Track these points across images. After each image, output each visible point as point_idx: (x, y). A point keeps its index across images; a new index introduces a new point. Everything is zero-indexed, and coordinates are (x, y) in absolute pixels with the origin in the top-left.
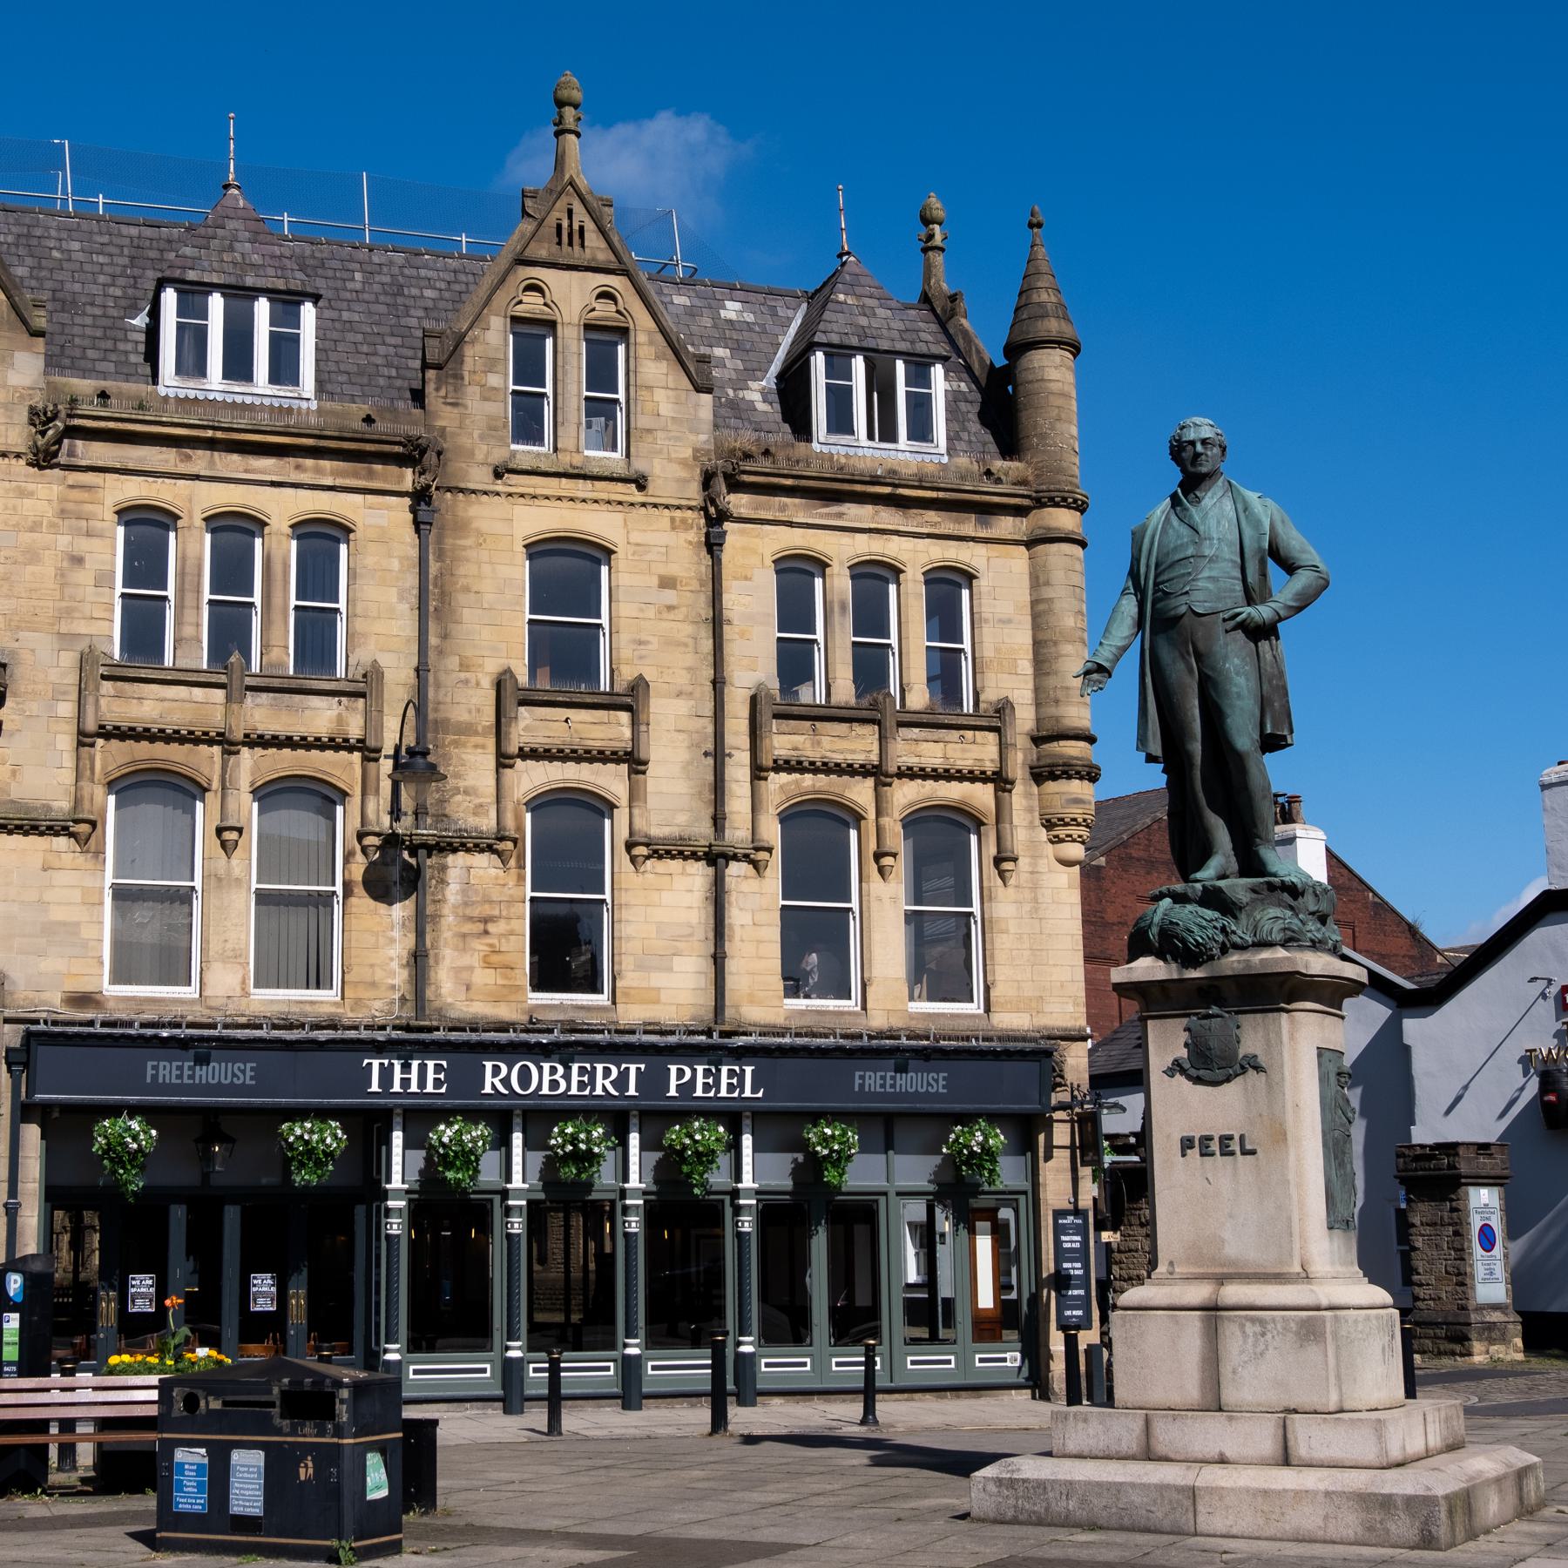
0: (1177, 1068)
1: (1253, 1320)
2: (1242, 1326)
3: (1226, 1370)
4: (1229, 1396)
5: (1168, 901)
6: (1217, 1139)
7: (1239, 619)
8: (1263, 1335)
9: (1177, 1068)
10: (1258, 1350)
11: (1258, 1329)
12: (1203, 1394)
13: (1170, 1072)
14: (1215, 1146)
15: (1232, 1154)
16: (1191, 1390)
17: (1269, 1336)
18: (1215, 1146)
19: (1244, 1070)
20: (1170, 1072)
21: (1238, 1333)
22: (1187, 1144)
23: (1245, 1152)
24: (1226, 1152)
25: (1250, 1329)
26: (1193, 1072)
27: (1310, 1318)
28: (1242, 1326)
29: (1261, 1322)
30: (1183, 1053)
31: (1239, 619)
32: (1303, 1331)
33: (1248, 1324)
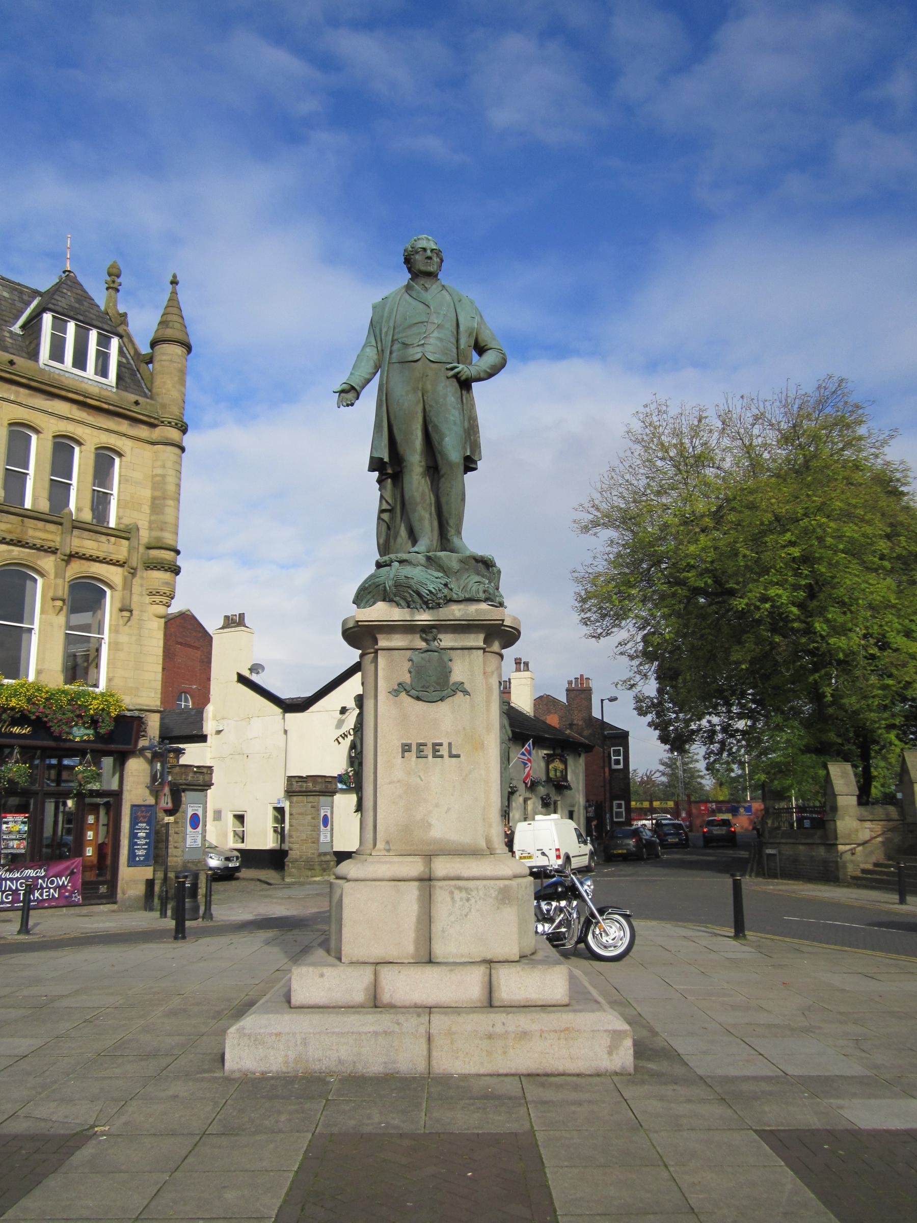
0: (401, 689)
1: (460, 889)
2: (452, 893)
3: (437, 928)
4: (440, 950)
5: (396, 564)
6: (430, 746)
7: (456, 370)
8: (468, 900)
9: (401, 689)
10: (464, 913)
11: (464, 895)
12: (417, 949)
13: (395, 693)
14: (428, 751)
15: (441, 757)
16: (407, 946)
17: (473, 900)
18: (428, 751)
19: (454, 693)
20: (395, 693)
21: (449, 899)
22: (406, 748)
23: (452, 756)
24: (436, 754)
25: (458, 895)
26: (413, 692)
27: (506, 886)
28: (452, 893)
29: (467, 890)
30: (407, 678)
31: (456, 370)
32: (500, 897)
33: (456, 892)
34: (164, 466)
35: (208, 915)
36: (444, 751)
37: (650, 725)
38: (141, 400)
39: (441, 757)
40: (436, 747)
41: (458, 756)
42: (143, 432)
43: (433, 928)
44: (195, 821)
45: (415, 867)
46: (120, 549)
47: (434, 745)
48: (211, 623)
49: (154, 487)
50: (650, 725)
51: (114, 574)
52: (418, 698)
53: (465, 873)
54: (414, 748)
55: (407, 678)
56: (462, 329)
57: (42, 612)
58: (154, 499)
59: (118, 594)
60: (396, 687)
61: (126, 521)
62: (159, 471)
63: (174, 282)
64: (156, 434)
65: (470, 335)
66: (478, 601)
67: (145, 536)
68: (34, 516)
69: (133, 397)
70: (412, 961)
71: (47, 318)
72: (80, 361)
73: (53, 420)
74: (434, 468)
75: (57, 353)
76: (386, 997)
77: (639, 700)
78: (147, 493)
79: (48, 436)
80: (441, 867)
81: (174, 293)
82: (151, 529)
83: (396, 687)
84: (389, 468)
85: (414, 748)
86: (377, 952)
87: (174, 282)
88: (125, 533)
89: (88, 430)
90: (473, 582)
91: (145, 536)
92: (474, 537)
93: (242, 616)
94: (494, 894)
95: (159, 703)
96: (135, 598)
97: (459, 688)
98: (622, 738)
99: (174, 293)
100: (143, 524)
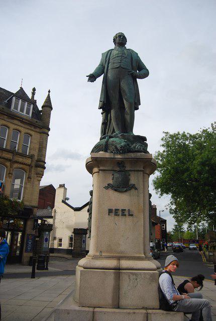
4: (123, 302)
11: (135, 277)
15: (125, 215)
16: (109, 300)
17: (138, 280)
18: (120, 213)
22: (110, 211)
24: (123, 215)
29: (135, 274)
32: (151, 278)
33: (131, 275)
34: (43, 139)
35: (47, 269)
36: (127, 213)
37: (173, 217)
38: (38, 121)
39: (125, 215)
40: (123, 210)
41: (132, 215)
42: (38, 130)
43: (121, 293)
44: (47, 240)
45: (112, 263)
46: (28, 161)
47: (122, 210)
48: (56, 186)
49: (40, 145)
50: (173, 217)
51: (27, 168)
52: (116, 190)
53: (135, 267)
54: (114, 211)
55: (111, 182)
56: (133, 59)
57: (6, 177)
58: (40, 148)
59: (27, 174)
60: (107, 185)
61: (31, 153)
62: (41, 141)
63: (49, 92)
64: (41, 131)
65: (137, 62)
66: (141, 152)
67: (36, 158)
68: (6, 150)
69: (36, 120)
70: (110, 307)
71: (14, 98)
72: (22, 110)
74: (122, 107)
75: (16, 108)
77: (171, 209)
78: (37, 146)
81: (49, 94)
82: (38, 156)
83: (107, 185)
84: (106, 106)
85: (114, 211)
86: (95, 302)
87: (49, 92)
88: (31, 157)
89: (23, 128)
90: (138, 146)
91: (36, 158)
92: (137, 131)
93: (64, 184)
94: (148, 277)
95: (37, 205)
96: (32, 175)
97: (133, 187)
98: (164, 222)
99: (49, 94)
100: (36, 155)
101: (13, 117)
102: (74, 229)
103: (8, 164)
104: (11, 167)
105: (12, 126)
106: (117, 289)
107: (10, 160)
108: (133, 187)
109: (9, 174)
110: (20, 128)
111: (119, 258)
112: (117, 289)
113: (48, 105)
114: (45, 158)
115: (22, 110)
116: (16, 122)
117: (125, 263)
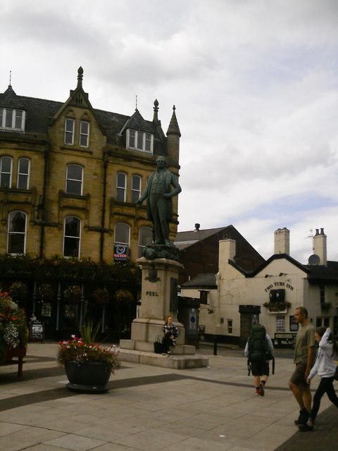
0: (147, 279)
3: (149, 334)
9: (147, 279)
16: (143, 338)
22: (147, 293)
30: (148, 276)
40: (153, 293)
55: (148, 276)
57: (131, 239)
68: (127, 205)
71: (128, 131)
72: (140, 146)
73: (132, 169)
75: (132, 144)
76: (137, 348)
79: (130, 175)
80: (151, 321)
89: (144, 171)
97: (159, 279)
101: (130, 158)
102: (240, 306)
103: (132, 221)
104: (135, 226)
105: (131, 171)
106: (147, 333)
107: (132, 217)
108: (159, 279)
109: (134, 234)
110: (141, 172)
111: (150, 319)
112: (147, 333)
113: (175, 129)
114: (177, 209)
115: (140, 146)
116: (135, 164)
117: (151, 321)
